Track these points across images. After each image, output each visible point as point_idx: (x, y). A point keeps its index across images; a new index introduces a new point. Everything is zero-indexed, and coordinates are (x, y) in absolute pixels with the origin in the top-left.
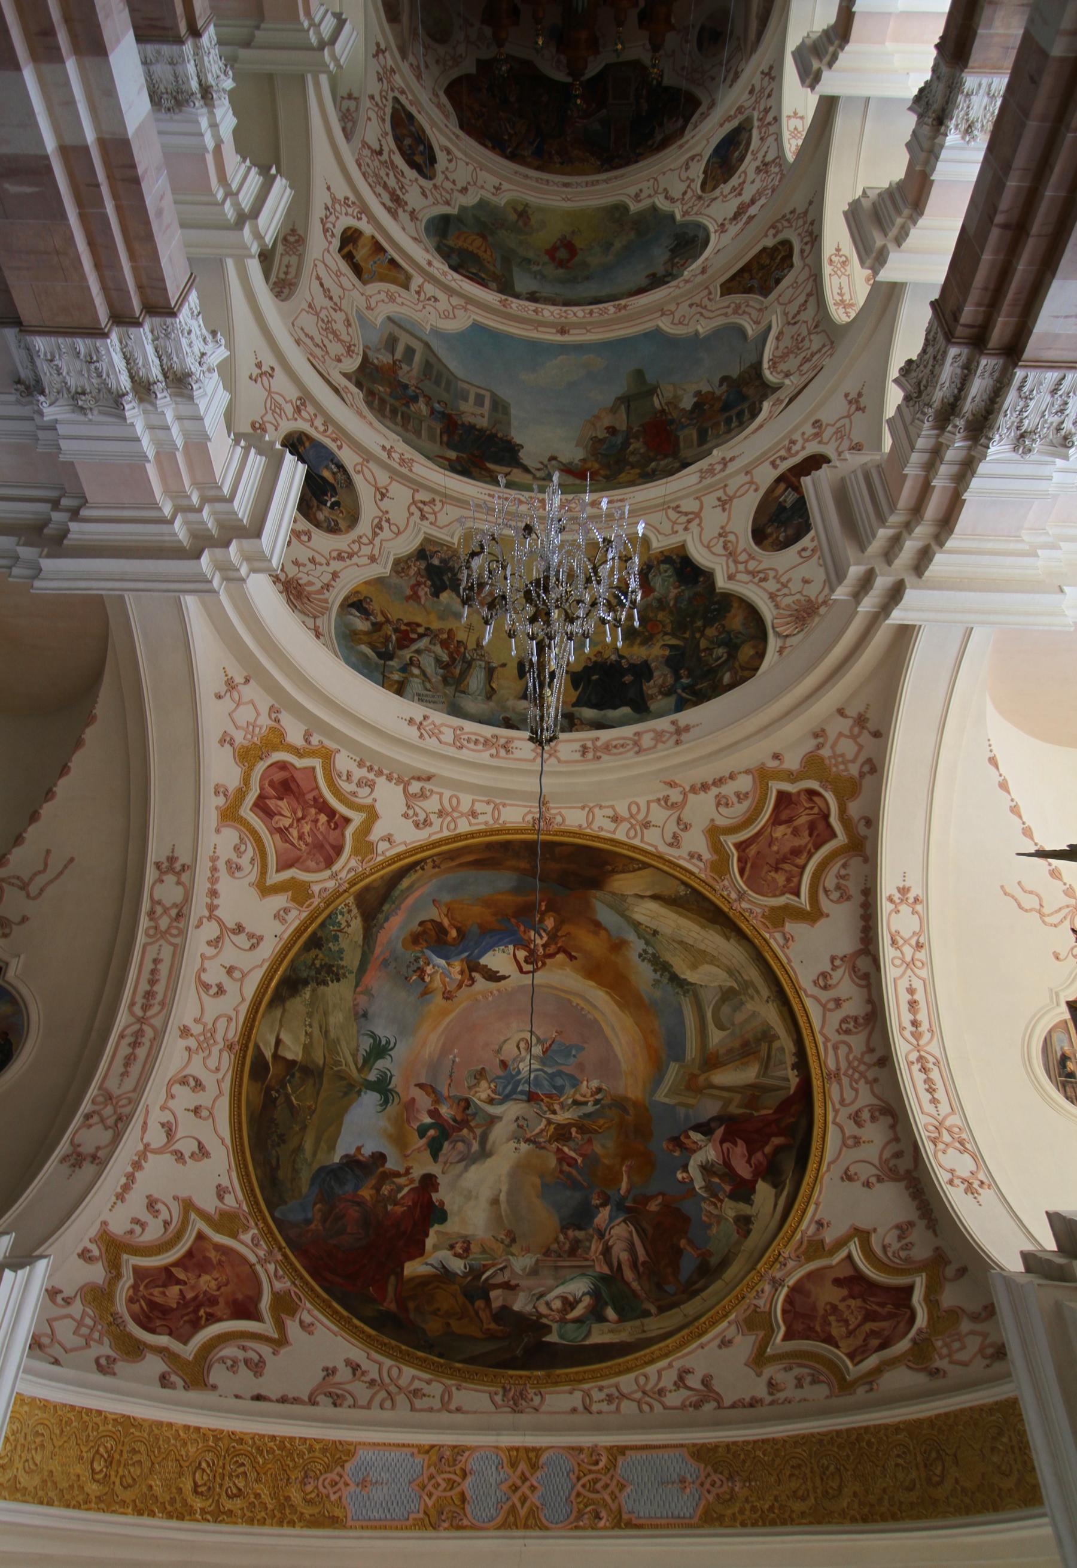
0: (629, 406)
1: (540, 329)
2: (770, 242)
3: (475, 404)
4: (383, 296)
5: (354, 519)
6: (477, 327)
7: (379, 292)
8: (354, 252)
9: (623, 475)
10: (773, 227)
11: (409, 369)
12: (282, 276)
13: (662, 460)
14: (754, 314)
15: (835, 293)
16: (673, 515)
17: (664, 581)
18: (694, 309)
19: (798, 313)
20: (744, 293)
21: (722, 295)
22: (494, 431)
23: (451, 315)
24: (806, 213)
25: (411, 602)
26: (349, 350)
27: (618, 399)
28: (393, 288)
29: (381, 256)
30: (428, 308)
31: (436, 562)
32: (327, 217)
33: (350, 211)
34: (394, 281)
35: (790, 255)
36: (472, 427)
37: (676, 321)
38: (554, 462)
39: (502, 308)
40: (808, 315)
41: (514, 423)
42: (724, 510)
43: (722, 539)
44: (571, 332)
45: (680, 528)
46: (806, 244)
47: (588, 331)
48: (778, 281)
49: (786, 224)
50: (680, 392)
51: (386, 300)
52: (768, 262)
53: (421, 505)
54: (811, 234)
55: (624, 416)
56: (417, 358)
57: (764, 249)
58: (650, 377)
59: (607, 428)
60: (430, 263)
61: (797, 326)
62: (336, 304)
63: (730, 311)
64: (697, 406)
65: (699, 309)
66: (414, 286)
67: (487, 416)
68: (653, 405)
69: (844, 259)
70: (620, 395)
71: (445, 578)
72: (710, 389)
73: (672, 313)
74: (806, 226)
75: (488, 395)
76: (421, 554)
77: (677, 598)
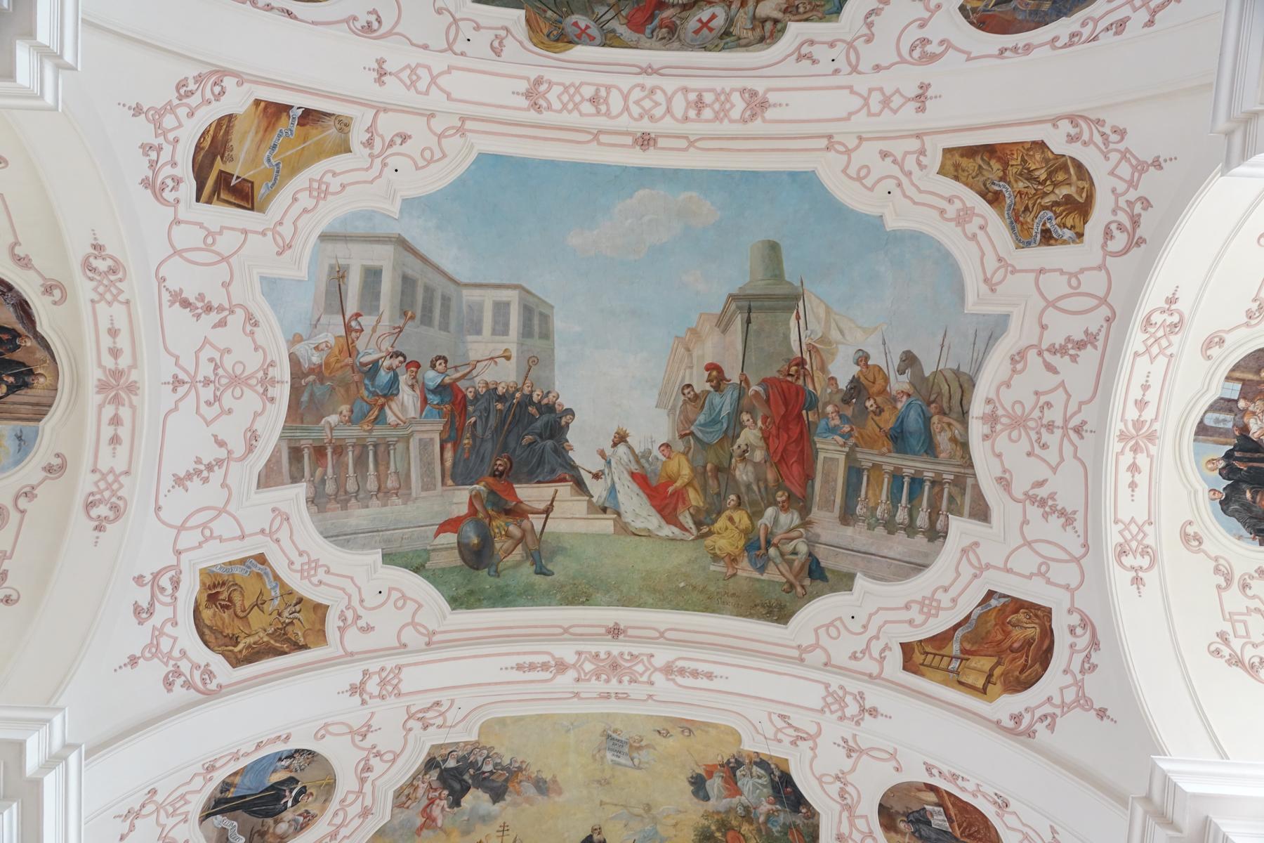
0: (749, 321)
1: (603, 138)
2: (1058, 145)
3: (494, 332)
4: (305, 201)
5: (329, 786)
6: (489, 162)
7: (295, 200)
8: (228, 168)
9: (722, 522)
10: (1072, 119)
11: (374, 319)
12: (108, 362)
13: (785, 509)
14: (991, 263)
15: (1131, 403)
16: (780, 723)
17: (755, 787)
18: (888, 167)
19: (1061, 350)
20: (983, 196)
21: (942, 172)
22: (526, 390)
23: (438, 155)
24: (1141, 168)
25: (425, 832)
26: (267, 382)
27: (733, 297)
28: (316, 170)
29: (285, 124)
30: (393, 162)
31: (451, 763)
32: (153, 164)
33: (195, 100)
34: (321, 153)
35: (1081, 208)
36: (492, 393)
37: (852, 171)
38: (622, 449)
39: (532, 116)
40: (1077, 373)
41: (560, 354)
42: (849, 756)
43: (838, 784)
44: (662, 142)
45: (787, 740)
46: (1121, 227)
47: (691, 144)
48: (1047, 237)
49: (1097, 138)
50: (834, 335)
51: (310, 203)
52: (1042, 174)
53: (420, 715)
54: (1135, 222)
55: (739, 347)
56: (388, 285)
57: (1041, 145)
58: (791, 271)
59: (711, 367)
60: (382, 74)
61: (1053, 380)
62: (221, 309)
63: (951, 211)
64: (857, 389)
65: (895, 170)
66: (357, 136)
67: (514, 354)
68: (787, 337)
69: (1176, 318)
70: (735, 291)
71: (466, 777)
72: (884, 367)
73: (848, 152)
74: (1132, 195)
75: (512, 296)
76: (431, 764)
77: (769, 816)
